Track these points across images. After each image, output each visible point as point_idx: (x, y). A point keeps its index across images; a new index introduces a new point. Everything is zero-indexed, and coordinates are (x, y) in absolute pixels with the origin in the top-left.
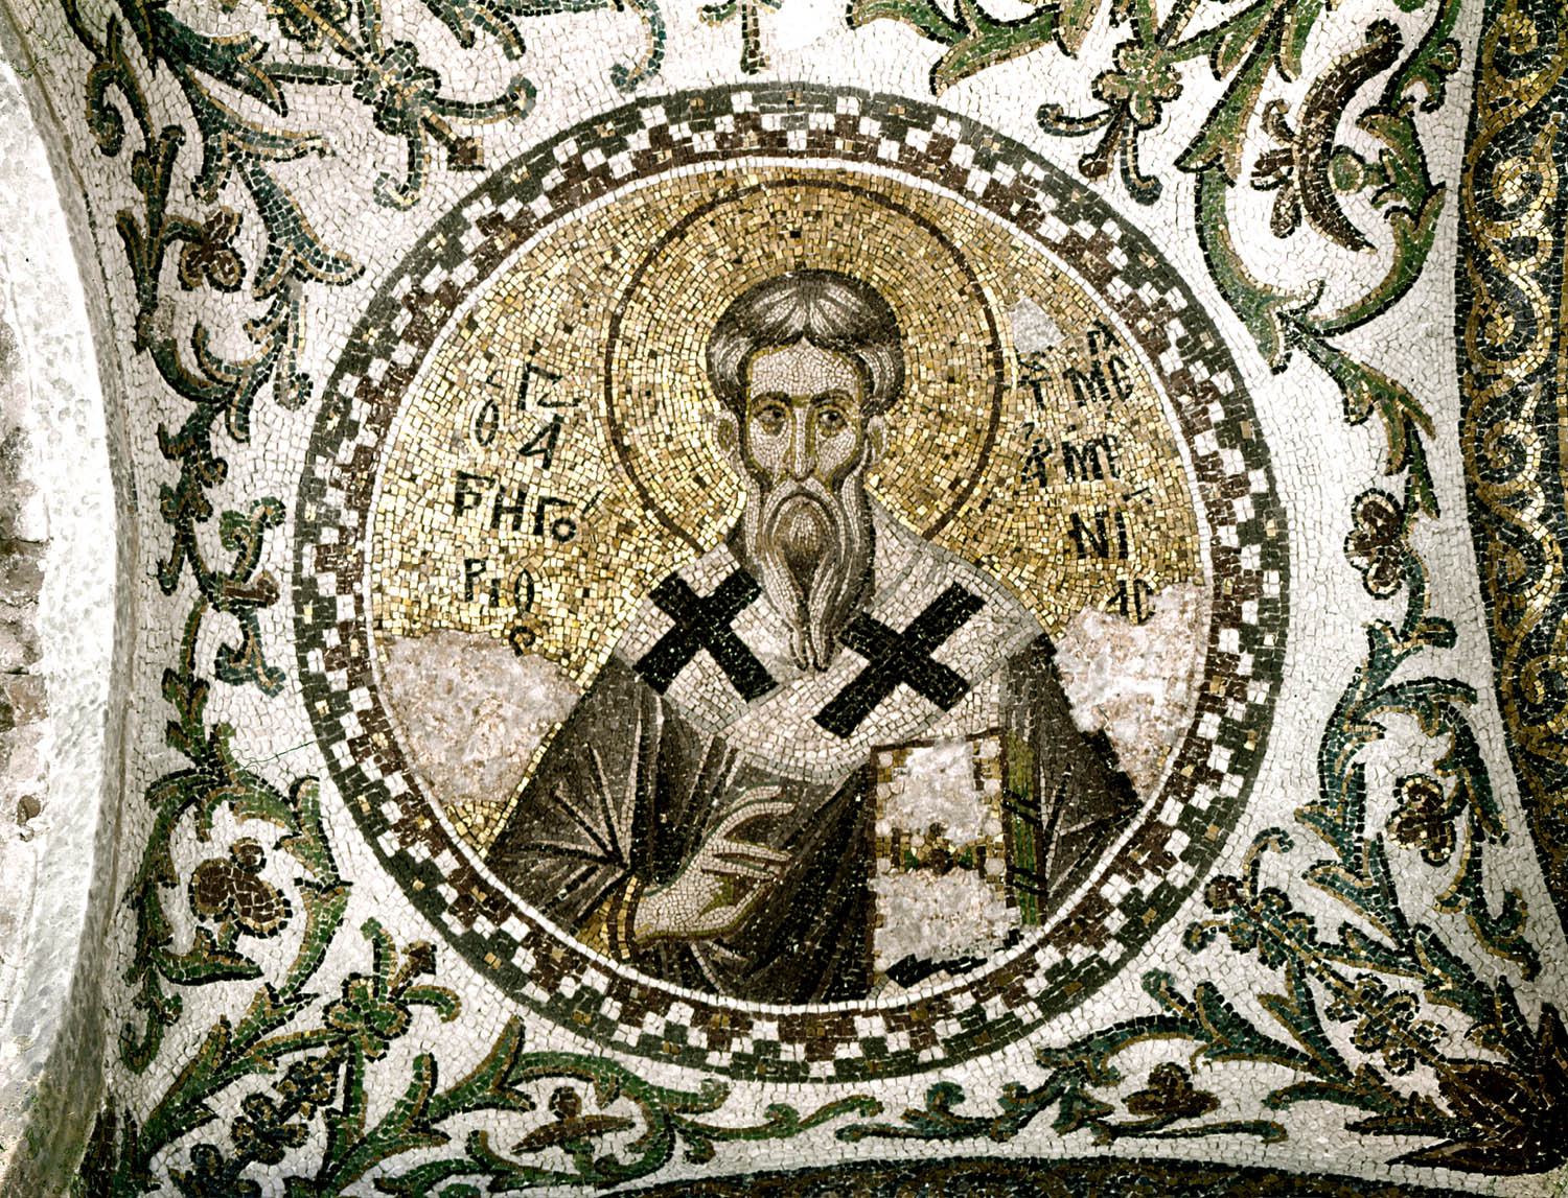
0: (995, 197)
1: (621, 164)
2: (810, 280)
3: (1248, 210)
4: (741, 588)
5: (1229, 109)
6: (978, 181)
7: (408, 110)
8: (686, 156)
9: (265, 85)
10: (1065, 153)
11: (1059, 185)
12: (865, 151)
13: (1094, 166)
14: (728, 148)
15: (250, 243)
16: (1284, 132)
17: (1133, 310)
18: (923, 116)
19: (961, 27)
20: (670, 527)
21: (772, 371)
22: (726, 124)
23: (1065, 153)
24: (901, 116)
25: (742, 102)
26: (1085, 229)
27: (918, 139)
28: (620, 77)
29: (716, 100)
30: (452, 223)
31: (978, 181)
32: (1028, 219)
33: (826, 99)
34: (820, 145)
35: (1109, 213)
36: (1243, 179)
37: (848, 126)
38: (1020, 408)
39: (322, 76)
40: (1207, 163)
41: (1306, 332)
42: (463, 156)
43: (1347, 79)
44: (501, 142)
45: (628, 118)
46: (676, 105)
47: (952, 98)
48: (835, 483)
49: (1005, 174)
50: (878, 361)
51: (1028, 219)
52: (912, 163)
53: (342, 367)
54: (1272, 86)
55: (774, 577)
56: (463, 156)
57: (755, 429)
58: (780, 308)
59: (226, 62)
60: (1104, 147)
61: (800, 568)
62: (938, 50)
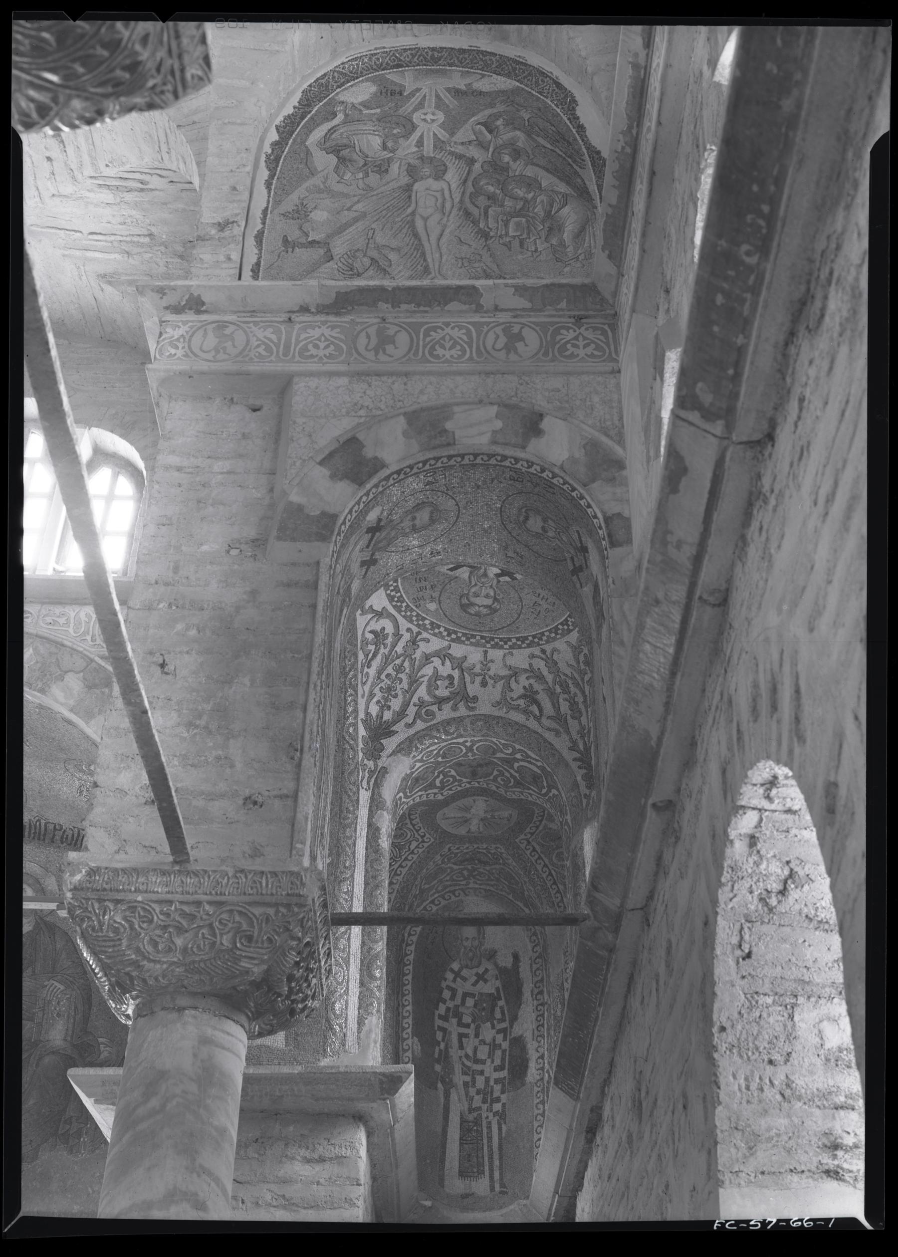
0: (439, 627)
1: (514, 641)
2: (478, 615)
3: (390, 629)
4: (498, 576)
5: (394, 646)
6: (442, 629)
7: (552, 664)
8: (501, 640)
9: (573, 678)
10: (425, 635)
11: (426, 630)
12: (464, 635)
13: (419, 633)
14: (492, 639)
15: (582, 658)
16: (384, 644)
17: (412, 610)
18: (453, 640)
19: (444, 656)
20: (513, 587)
21: (489, 602)
22: (492, 643)
23: (425, 635)
24: (457, 640)
25: (488, 645)
26: (421, 622)
27: (454, 636)
28: (512, 654)
29: (493, 647)
30: (547, 642)
31: (442, 629)
32: (432, 623)
33: (472, 644)
34: (474, 636)
35: (416, 625)
36: (391, 635)
37: (468, 639)
38: (436, 594)
39: (565, 674)
40: (398, 636)
41: (379, 615)
42: (543, 651)
43: (374, 656)
44: (536, 651)
45: (511, 647)
46: (501, 647)
47: (447, 643)
48: (476, 585)
49: (437, 631)
50: (465, 601)
51: (432, 623)
52: (455, 632)
53: (572, 630)
54: (386, 651)
55: (491, 575)
56: (543, 651)
57: (492, 594)
58: (485, 611)
59: (577, 685)
60: (416, 637)
61: (485, 575)
62: (450, 652)
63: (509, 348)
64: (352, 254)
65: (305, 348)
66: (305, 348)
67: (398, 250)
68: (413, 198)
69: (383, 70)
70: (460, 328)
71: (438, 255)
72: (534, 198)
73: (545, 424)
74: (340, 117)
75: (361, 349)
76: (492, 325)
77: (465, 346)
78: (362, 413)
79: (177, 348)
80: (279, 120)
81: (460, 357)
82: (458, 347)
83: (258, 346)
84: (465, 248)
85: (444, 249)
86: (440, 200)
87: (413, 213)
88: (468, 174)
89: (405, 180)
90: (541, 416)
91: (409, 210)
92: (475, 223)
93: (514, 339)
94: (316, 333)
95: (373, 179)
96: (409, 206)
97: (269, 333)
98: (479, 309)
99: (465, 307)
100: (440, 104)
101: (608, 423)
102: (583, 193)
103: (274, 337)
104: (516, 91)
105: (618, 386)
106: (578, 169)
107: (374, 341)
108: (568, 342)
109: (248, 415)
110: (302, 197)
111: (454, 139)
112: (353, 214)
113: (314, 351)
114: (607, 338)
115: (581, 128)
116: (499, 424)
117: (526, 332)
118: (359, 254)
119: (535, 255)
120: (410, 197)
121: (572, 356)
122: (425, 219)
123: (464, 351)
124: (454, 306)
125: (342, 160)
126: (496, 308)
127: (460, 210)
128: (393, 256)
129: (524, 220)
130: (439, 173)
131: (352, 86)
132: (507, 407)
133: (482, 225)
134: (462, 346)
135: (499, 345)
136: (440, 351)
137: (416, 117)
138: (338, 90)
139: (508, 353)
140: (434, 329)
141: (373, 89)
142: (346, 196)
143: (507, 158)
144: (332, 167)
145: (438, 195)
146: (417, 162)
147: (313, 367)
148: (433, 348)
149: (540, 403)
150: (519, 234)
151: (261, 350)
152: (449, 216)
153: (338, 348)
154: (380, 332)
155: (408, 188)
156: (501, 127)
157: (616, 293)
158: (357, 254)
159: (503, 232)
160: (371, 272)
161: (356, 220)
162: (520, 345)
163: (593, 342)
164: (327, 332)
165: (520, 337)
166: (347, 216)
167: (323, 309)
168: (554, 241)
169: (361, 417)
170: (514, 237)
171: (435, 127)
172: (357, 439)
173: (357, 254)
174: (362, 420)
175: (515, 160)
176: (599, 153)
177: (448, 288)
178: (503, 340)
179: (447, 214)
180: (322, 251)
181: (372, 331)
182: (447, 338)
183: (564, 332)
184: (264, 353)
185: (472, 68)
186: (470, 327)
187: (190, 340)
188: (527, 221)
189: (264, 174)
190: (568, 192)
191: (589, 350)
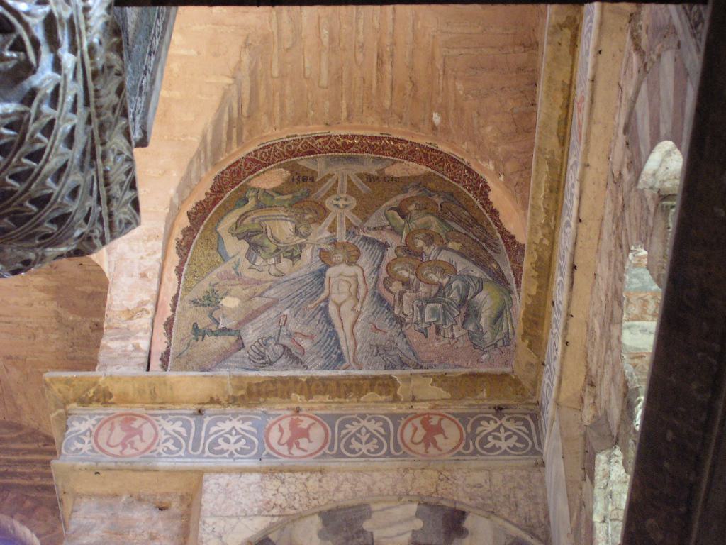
63: (428, 441)
64: (264, 343)
65: (215, 443)
66: (215, 443)
68: (326, 283)
69: (296, 156)
70: (377, 420)
71: (351, 343)
72: (449, 284)
73: (468, 523)
74: (252, 202)
75: (274, 442)
76: (410, 416)
77: (382, 439)
78: (275, 512)
79: (83, 442)
80: (190, 206)
81: (377, 451)
82: (375, 441)
83: (166, 440)
84: (379, 335)
85: (358, 335)
86: (353, 287)
87: (326, 300)
89: (318, 265)
90: (463, 515)
91: (323, 296)
92: (390, 308)
93: (432, 432)
94: (227, 426)
95: (285, 264)
96: (322, 292)
97: (178, 426)
98: (396, 399)
99: (383, 398)
100: (352, 190)
101: (534, 521)
102: (499, 278)
103: (183, 431)
104: (427, 177)
105: (542, 480)
106: (493, 254)
107: (287, 434)
108: (489, 434)
109: (156, 514)
110: (213, 283)
111: (366, 224)
112: (265, 301)
113: (224, 446)
114: (529, 428)
115: (494, 213)
116: (419, 524)
117: (445, 423)
118: (271, 342)
119: (452, 342)
120: (323, 283)
121: (494, 449)
122: (339, 306)
123: (380, 444)
124: (370, 396)
125: (255, 247)
126: (414, 399)
127: (374, 295)
129: (439, 306)
130: (352, 259)
131: (263, 172)
132: (429, 507)
133: (397, 312)
134: (377, 438)
135: (418, 438)
136: (356, 445)
137: (328, 203)
138: (251, 176)
139: (427, 446)
140: (350, 421)
141: (286, 174)
142: (258, 283)
143: (420, 243)
144: (244, 252)
146: (328, 247)
147: (225, 462)
148: (348, 443)
149: (462, 498)
150: (434, 319)
151: (170, 444)
152: (362, 303)
153: (250, 442)
154: (293, 425)
155: (321, 274)
156: (415, 212)
157: (536, 384)
158: (270, 342)
159: (419, 319)
160: (283, 361)
161: (268, 307)
162: (439, 438)
163: (515, 433)
164: (239, 425)
165: (439, 430)
166: (258, 302)
167: (233, 401)
168: (471, 327)
169: (273, 516)
170: (430, 324)
171: (348, 213)
172: (270, 540)
173: (270, 342)
174: (275, 520)
175: (428, 245)
176: (513, 237)
177: (364, 378)
178: (421, 432)
179: (361, 300)
180: (232, 339)
181: (285, 424)
182: (364, 431)
183: (484, 423)
184: (173, 448)
185: (383, 154)
186: (387, 419)
187: (97, 434)
188: (443, 307)
189: (174, 259)
190: (483, 277)
191: (512, 442)
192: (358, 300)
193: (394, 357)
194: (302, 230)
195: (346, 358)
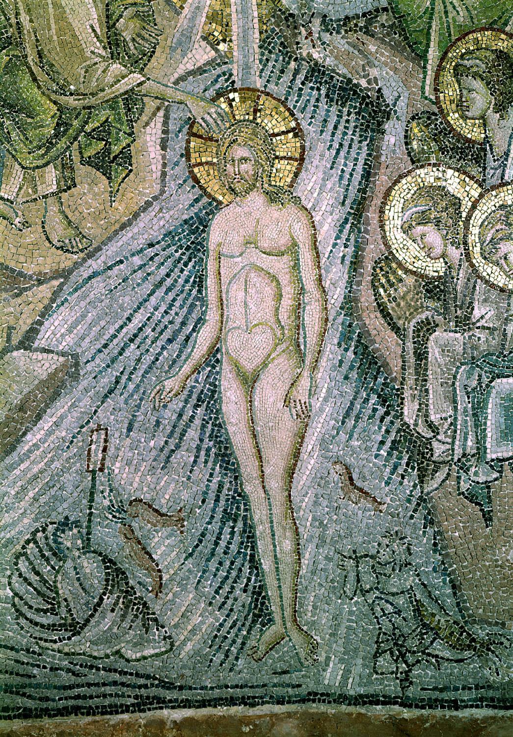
67: (175, 519)
68: (210, 282)
71: (287, 545)
84: (359, 512)
85: (304, 502)
86: (288, 291)
88: (367, 175)
91: (204, 338)
96: (200, 321)
120: (200, 282)
127: (345, 338)
128: (165, 546)
133: (410, 411)
145: (280, 266)
152: (314, 368)
155: (198, 226)
158: (68, 539)
173: (68, 539)
179: (308, 359)
192: (302, 357)
193: (401, 601)
194: (127, 28)
195: (277, 617)
